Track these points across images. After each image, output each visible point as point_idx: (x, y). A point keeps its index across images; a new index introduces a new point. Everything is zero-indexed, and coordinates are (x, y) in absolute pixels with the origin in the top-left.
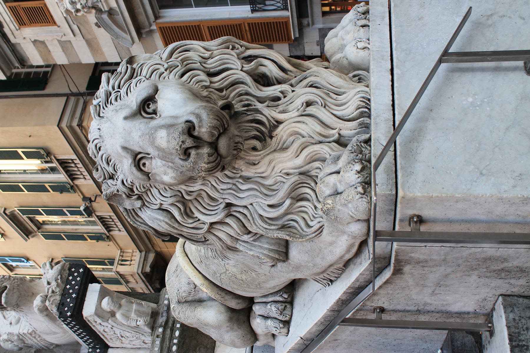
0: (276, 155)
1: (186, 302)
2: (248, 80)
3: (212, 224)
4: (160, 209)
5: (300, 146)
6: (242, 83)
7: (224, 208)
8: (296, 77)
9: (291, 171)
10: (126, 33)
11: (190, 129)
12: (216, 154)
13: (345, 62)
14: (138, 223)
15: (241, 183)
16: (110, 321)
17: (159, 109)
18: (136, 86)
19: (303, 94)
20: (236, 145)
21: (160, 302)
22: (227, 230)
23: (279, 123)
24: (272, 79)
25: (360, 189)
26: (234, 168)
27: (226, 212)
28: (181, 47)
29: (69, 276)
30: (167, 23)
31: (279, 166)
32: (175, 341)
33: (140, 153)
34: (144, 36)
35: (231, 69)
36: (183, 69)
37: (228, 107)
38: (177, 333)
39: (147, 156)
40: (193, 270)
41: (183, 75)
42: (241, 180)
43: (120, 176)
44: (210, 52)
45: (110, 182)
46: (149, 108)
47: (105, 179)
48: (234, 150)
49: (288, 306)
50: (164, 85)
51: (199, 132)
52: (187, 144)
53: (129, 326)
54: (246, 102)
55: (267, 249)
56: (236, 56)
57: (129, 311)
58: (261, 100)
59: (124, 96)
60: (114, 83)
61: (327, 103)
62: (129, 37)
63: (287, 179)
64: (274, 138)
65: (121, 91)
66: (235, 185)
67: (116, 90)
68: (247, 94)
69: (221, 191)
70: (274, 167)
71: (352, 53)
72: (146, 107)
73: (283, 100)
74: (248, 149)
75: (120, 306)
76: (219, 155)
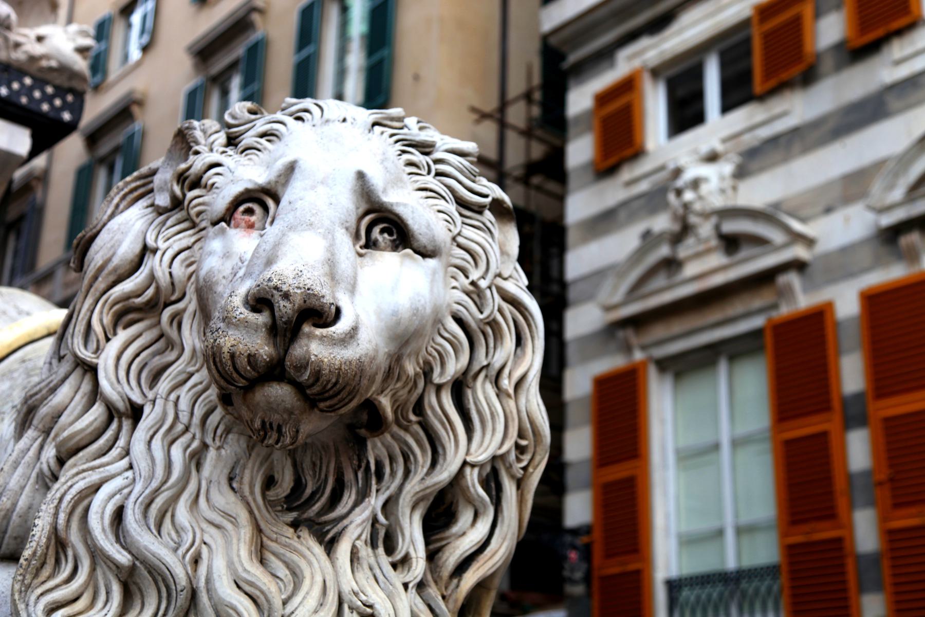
0: (246, 532)
3: (91, 370)
5: (262, 592)
7: (130, 400)
8: (444, 597)
9: (203, 570)
15: (188, 446)
17: (377, 254)
18: (439, 211)
20: (275, 427)
22: (74, 409)
23: (330, 546)
26: (228, 431)
27: (121, 405)
28: (529, 325)
29: (56, 87)
35: (470, 439)
36: (473, 324)
37: (373, 420)
39: (269, 219)
40: (9, 346)
42: (195, 444)
43: (231, 159)
44: (511, 391)
45: (221, 138)
46: (382, 231)
47: (230, 126)
48: (263, 423)
50: (434, 273)
51: (310, 336)
52: (282, 303)
54: (387, 470)
55: (14, 505)
58: (389, 506)
59: (417, 181)
63: (184, 557)
64: (291, 530)
65: (430, 178)
66: (187, 429)
67: (433, 167)
69: (173, 397)
70: (218, 527)
74: (271, 468)
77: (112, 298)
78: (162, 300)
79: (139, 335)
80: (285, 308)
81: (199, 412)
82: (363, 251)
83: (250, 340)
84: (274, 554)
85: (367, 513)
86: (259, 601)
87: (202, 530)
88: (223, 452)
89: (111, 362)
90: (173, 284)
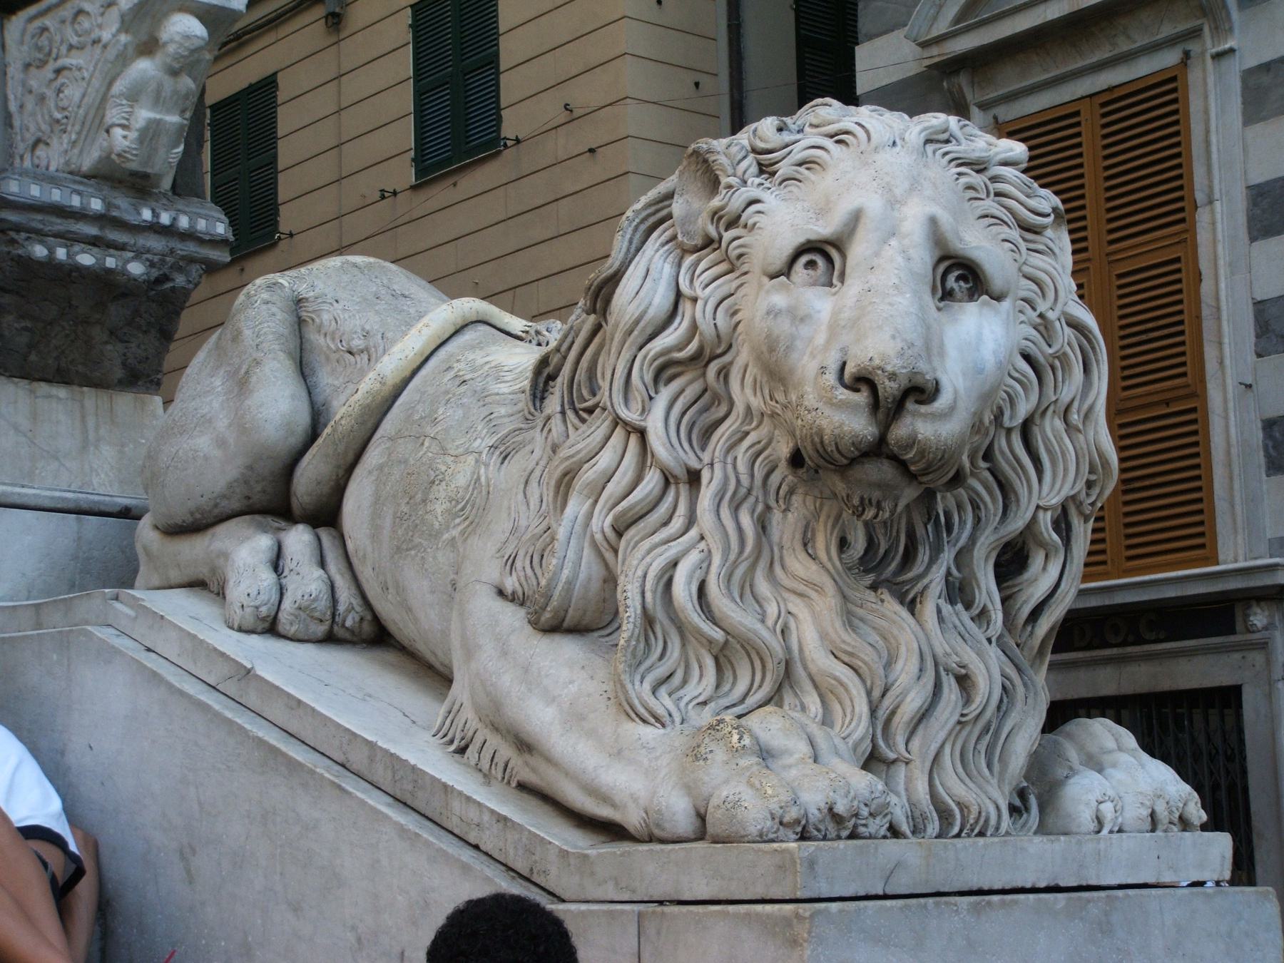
1: (300, 323)
2: (1017, 524)
3: (642, 433)
4: (679, 295)
8: (1018, 645)
11: (920, 391)
12: (857, 453)
13: (1061, 772)
16: (123, 38)
17: (956, 305)
19: (988, 668)
20: (874, 502)
21: (180, 204)
22: (625, 474)
23: (912, 606)
24: (1014, 586)
25: (793, 814)
26: (791, 492)
31: (806, 609)
32: (61, 253)
33: (844, 256)
36: (1042, 359)
39: (836, 273)
41: (1027, 357)
42: (760, 507)
45: (750, 163)
46: (958, 279)
48: (862, 499)
49: (321, 629)
53: (104, 99)
55: (575, 575)
56: (1072, 493)
57: (158, 101)
61: (968, 729)
70: (801, 595)
71: (1084, 793)
72: (959, 276)
73: (966, 616)
74: (843, 530)
75: (174, 73)
76: (853, 461)
77: (652, 354)
78: (707, 352)
79: (682, 391)
80: (889, 388)
81: (759, 474)
82: (942, 304)
83: (850, 421)
84: (862, 620)
85: (943, 570)
86: (861, 671)
87: (784, 600)
88: (790, 515)
89: (660, 425)
90: (718, 336)
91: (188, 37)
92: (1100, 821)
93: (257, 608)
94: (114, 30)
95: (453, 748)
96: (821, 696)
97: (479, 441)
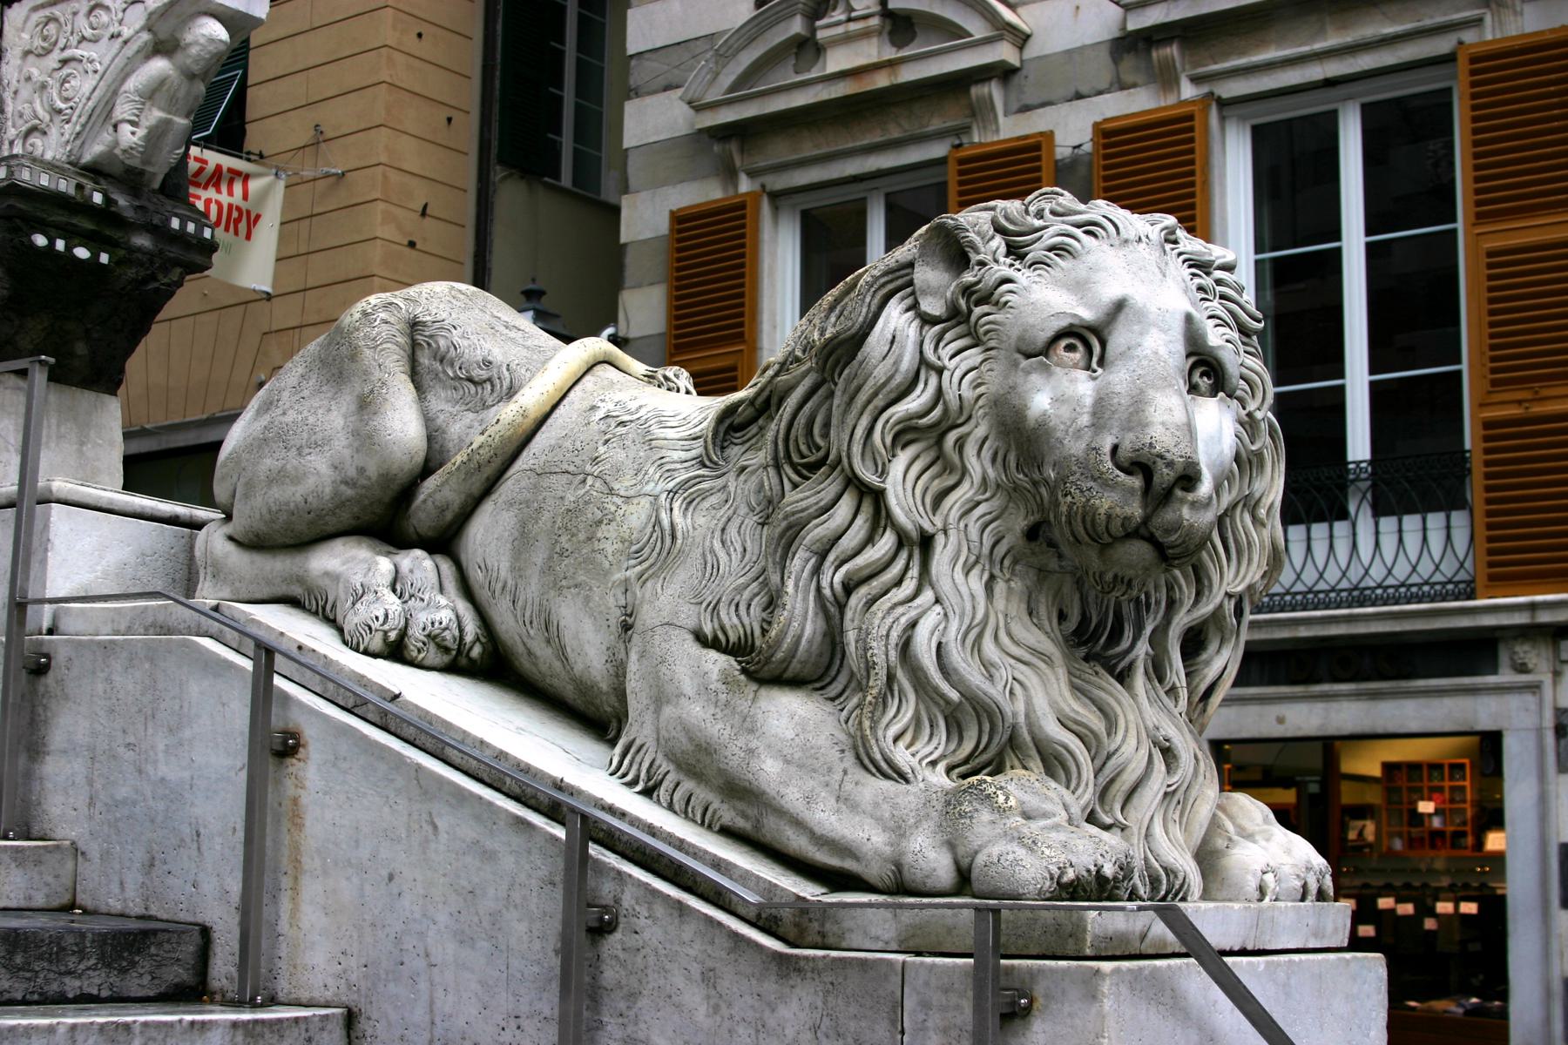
1: (414, 345)
2: (1206, 609)
3: (878, 496)
6: (1199, 594)
10: (732, 89)
14: (868, 300)
16: (145, 36)
30: (757, 230)
33: (1103, 344)
34: (716, 148)
38: (82, 253)
39: (1095, 359)
42: (986, 576)
43: (1023, 277)
46: (1202, 375)
48: (1116, 576)
49: (446, 659)
51: (1182, 501)
52: (1165, 471)
53: (115, 93)
55: (803, 630)
60: (1227, 285)
62: (714, 95)
68: (1172, 605)
72: (1206, 371)
80: (1164, 475)
81: (988, 541)
88: (1013, 584)
90: (961, 408)
91: (212, 40)
92: (1262, 891)
93: (386, 633)
94: (137, 26)
95: (639, 788)
96: (1043, 760)
97: (652, 484)
